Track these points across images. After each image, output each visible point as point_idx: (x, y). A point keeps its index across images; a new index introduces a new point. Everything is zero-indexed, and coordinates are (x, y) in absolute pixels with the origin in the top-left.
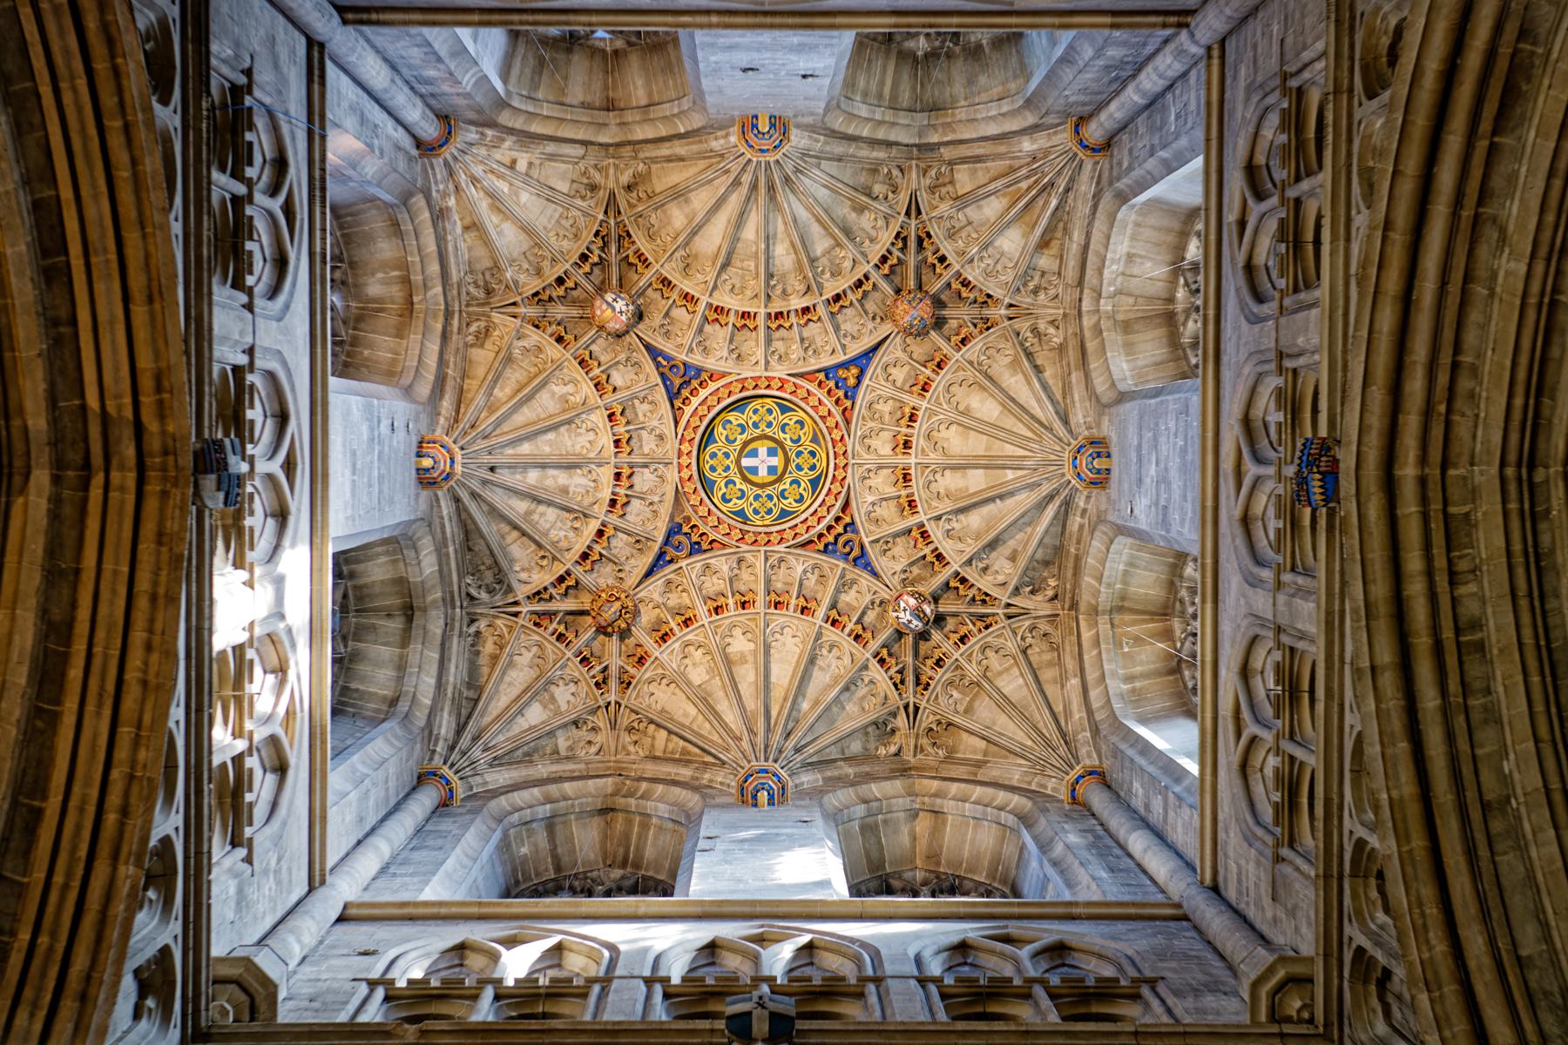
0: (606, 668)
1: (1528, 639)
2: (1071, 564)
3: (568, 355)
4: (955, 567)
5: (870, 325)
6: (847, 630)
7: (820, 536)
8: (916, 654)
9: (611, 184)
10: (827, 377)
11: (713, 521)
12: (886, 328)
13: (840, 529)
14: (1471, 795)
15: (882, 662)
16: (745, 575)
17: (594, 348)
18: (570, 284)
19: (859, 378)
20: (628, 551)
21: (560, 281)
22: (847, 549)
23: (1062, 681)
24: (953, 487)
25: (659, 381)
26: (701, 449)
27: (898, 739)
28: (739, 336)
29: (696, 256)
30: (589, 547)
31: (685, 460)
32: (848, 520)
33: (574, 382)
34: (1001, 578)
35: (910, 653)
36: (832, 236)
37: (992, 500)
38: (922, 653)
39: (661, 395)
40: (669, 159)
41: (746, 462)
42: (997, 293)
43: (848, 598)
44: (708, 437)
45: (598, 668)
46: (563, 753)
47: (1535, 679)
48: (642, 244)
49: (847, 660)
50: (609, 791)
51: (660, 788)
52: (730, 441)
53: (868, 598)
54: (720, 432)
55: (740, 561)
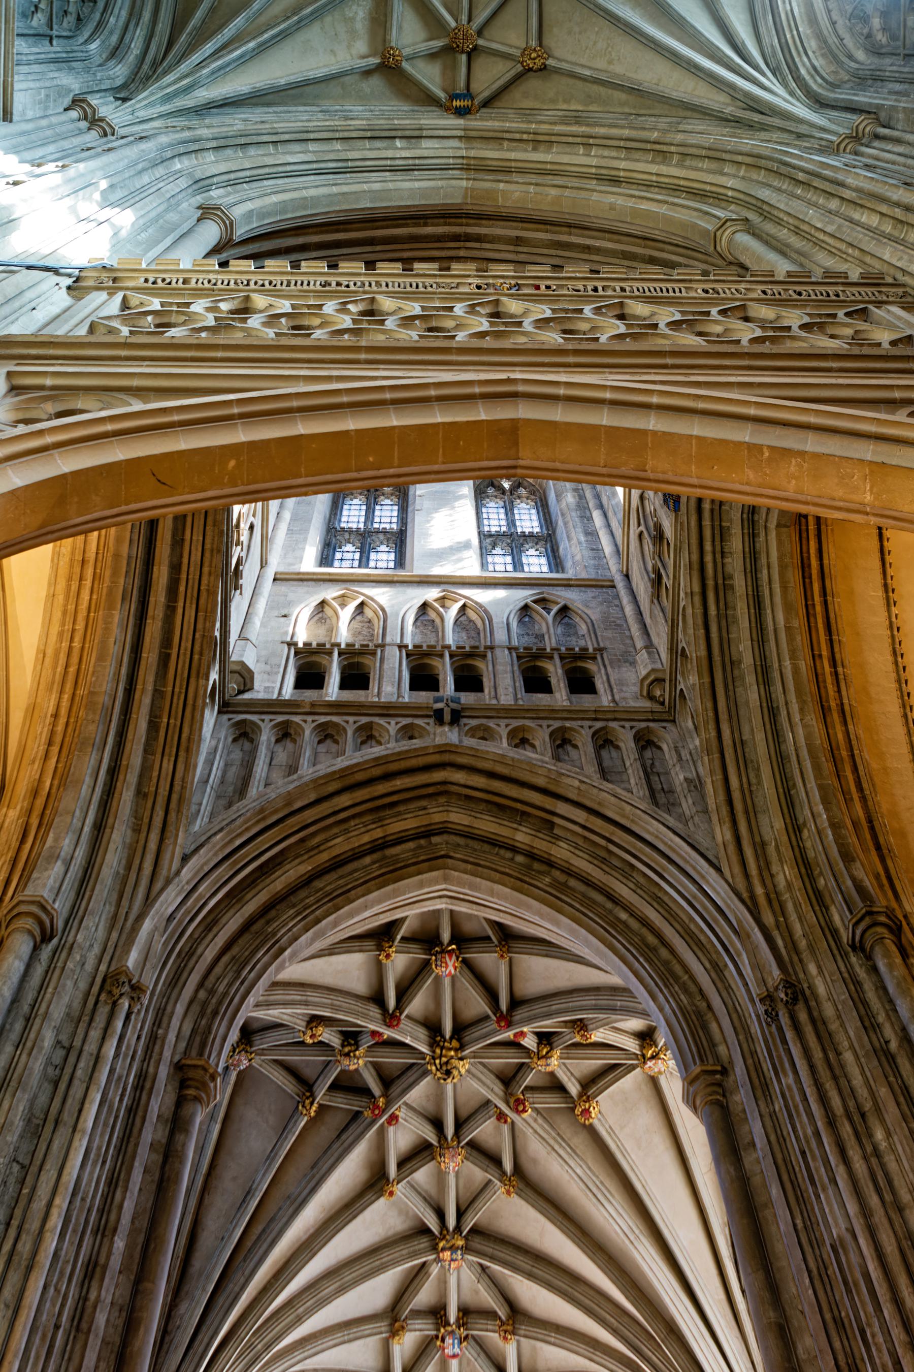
1: (750, 593)
14: (727, 659)
47: (752, 611)
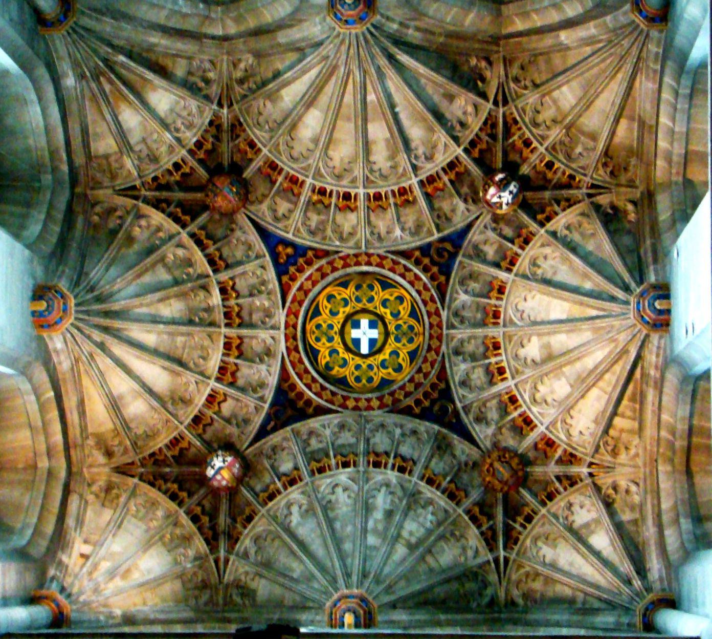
0: (558, 478)
2: (455, 43)
4: (460, 151)
5: (238, 233)
7: (433, 278)
8: (543, 188)
9: (106, 470)
10: (286, 272)
11: (419, 378)
12: (241, 219)
13: (426, 261)
15: (549, 219)
16: (470, 348)
18: (198, 510)
19: (287, 243)
20: (447, 458)
21: (195, 519)
22: (446, 254)
23: (564, 49)
25: (288, 428)
27: (620, 204)
28: (248, 353)
30: (443, 492)
31: (362, 404)
32: (417, 254)
33: (289, 506)
34: (470, 109)
35: (539, 195)
36: (154, 265)
37: (395, 116)
38: (541, 183)
39: (302, 426)
40: (82, 413)
41: (365, 349)
42: (208, 117)
43: (490, 251)
44: (342, 382)
45: (557, 484)
46: (637, 515)
48: (162, 441)
49: (547, 250)
50: (669, 468)
51: (665, 417)
55: (457, 353)
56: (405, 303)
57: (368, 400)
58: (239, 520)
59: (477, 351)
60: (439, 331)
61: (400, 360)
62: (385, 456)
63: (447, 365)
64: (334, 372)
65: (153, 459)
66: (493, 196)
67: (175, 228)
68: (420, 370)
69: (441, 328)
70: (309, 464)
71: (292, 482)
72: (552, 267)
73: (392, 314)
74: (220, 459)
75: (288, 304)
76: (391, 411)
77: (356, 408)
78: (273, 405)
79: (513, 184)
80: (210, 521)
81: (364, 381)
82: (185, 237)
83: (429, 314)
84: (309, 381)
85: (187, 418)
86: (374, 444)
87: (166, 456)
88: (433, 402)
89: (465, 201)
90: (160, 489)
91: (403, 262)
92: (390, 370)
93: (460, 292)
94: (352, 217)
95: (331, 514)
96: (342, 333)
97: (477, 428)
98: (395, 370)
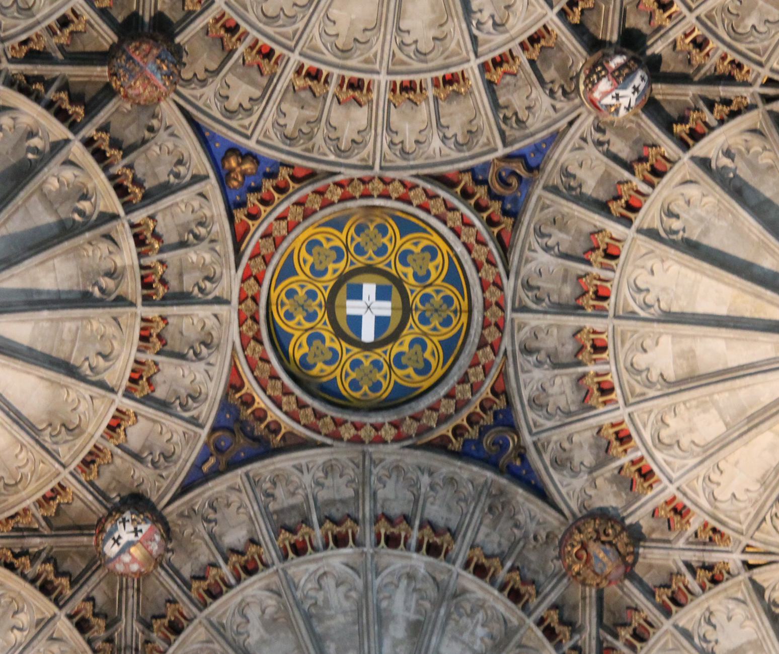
0: (688, 565)
3: (202, 616)
6: (644, 188)
7: (490, 223)
8: (683, 79)
10: (242, 204)
11: (464, 392)
12: (168, 111)
13: (481, 192)
15: (696, 136)
16: (549, 342)
17: (186, 572)
19: (247, 155)
20: (505, 525)
21: (82, 626)
22: (514, 181)
24: (429, 16)
25: (240, 471)
26: (343, 404)
29: (52, 413)
30: (501, 589)
31: (366, 433)
32: (467, 179)
38: (680, 68)
39: (263, 468)
41: (368, 334)
45: (689, 577)
49: (692, 192)
52: (334, 358)
53: (592, 151)
54: (320, 370)
55: (527, 351)
56: (439, 259)
57: (377, 427)
58: (156, 624)
59: (560, 348)
60: (500, 313)
61: (427, 355)
62: (404, 525)
63: (511, 370)
64: (315, 372)
65: (12, 523)
66: (606, 94)
67: (59, 130)
68: (464, 380)
69: (503, 309)
70: (277, 535)
71: (250, 570)
72: (701, 220)
73: (415, 275)
74: (130, 527)
75: (245, 260)
76: (413, 447)
77: (357, 440)
78: (214, 430)
79: (640, 73)
80: (107, 627)
81: (365, 388)
82: (77, 150)
83: (484, 286)
84: (278, 393)
85: (74, 458)
86: (385, 500)
87: (33, 515)
88: (483, 431)
89: (552, 93)
90: (23, 576)
91: (443, 194)
92: (410, 371)
93: (536, 246)
94: (360, 116)
95: (319, 629)
96: (330, 305)
97: (556, 476)
98: (418, 372)
